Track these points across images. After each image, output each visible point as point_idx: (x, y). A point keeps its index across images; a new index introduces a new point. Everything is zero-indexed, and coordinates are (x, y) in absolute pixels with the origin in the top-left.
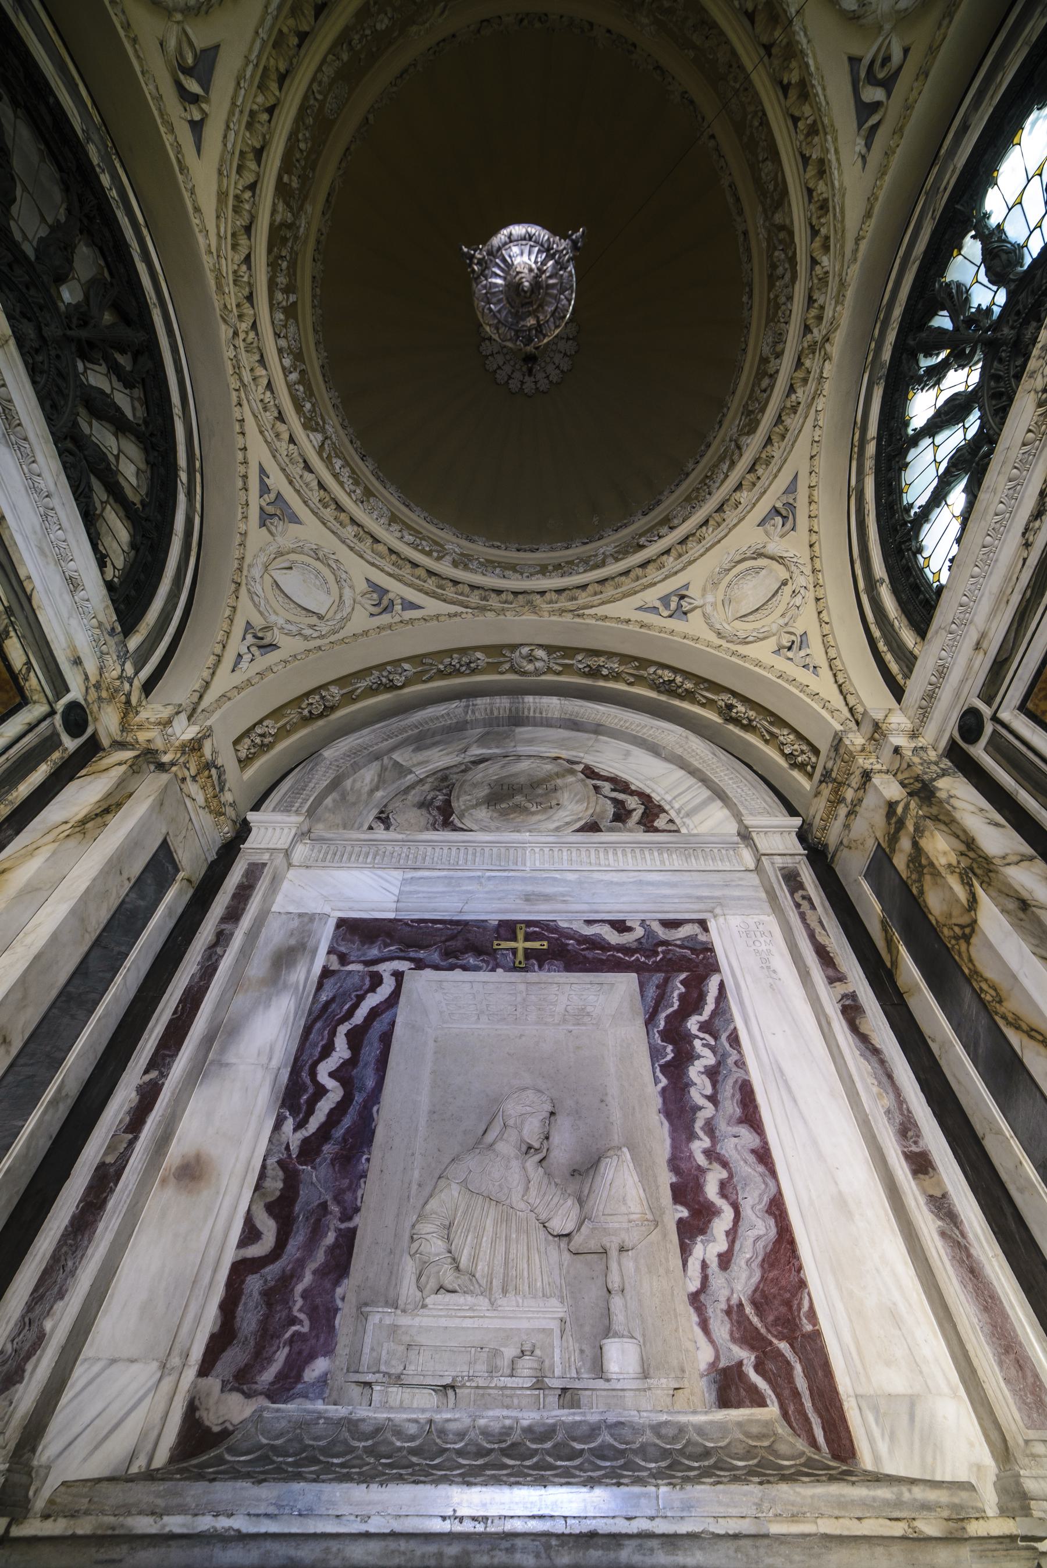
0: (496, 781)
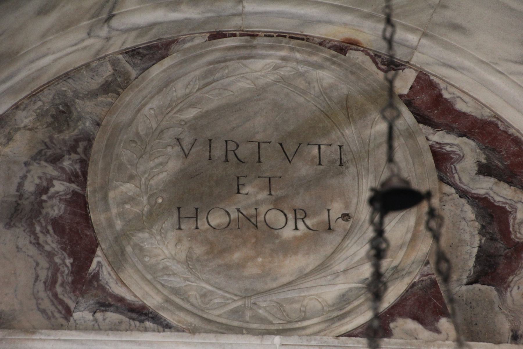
0: (193, 126)
